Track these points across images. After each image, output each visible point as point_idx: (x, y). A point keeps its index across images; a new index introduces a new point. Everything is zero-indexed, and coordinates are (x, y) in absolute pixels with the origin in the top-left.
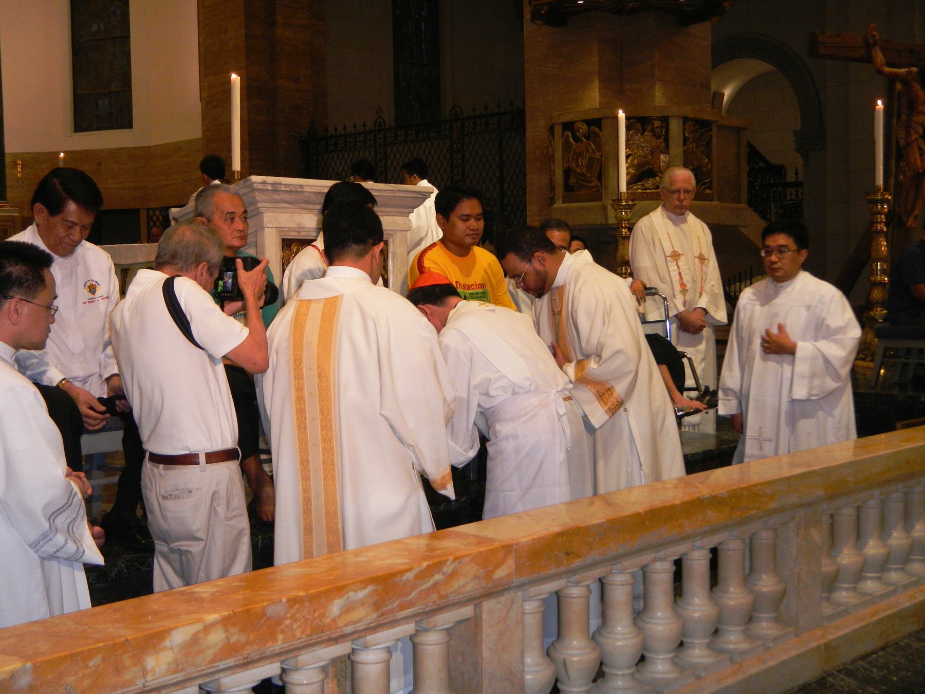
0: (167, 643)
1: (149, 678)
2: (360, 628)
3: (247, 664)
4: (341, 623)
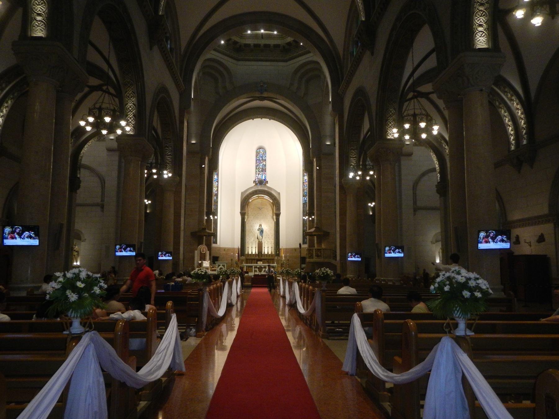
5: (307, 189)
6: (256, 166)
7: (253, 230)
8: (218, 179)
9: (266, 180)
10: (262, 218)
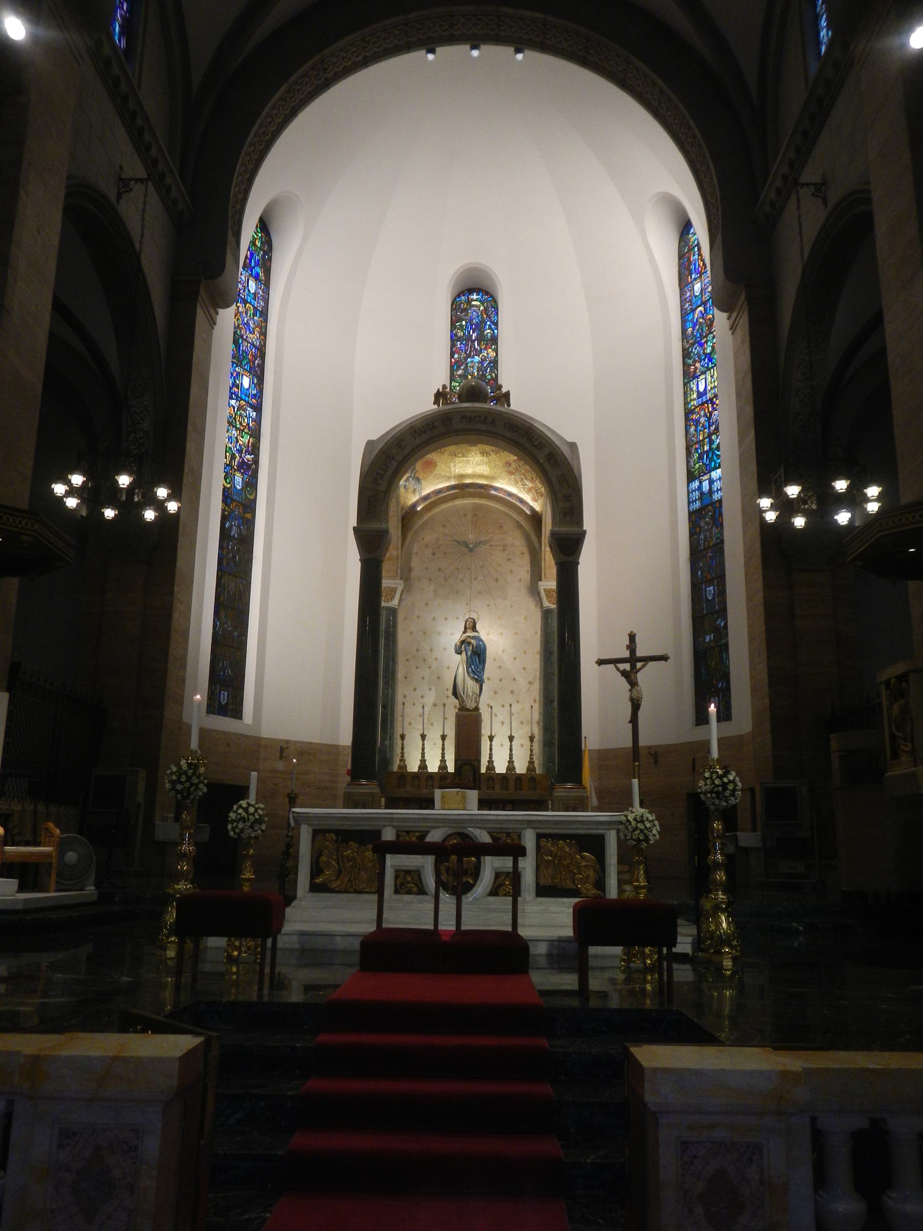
5: (710, 435)
6: (452, 366)
7: (431, 650)
8: (259, 396)
9: (500, 387)
10: (480, 593)
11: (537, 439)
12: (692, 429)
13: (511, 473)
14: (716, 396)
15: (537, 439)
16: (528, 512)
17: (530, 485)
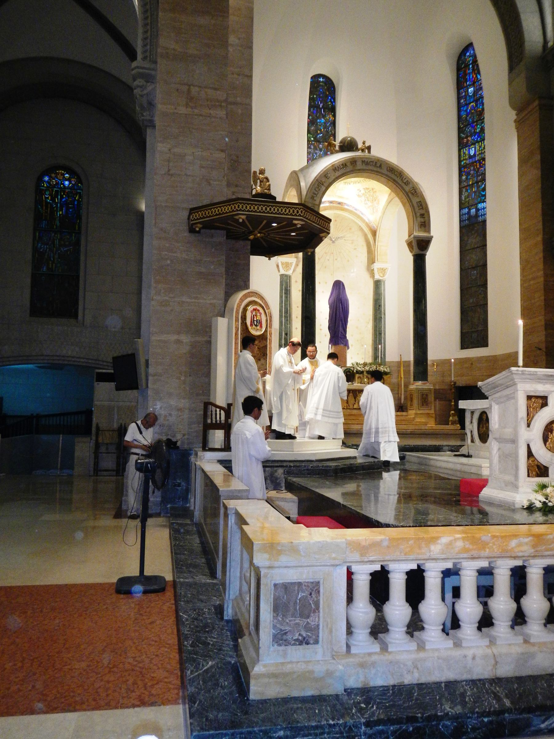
0: (439, 541)
1: (432, 553)
2: (526, 555)
3: (473, 558)
4: (516, 550)
11: (405, 179)
12: (464, 177)
13: (359, 196)
14: (484, 159)
15: (405, 179)
16: (367, 221)
17: (369, 204)
